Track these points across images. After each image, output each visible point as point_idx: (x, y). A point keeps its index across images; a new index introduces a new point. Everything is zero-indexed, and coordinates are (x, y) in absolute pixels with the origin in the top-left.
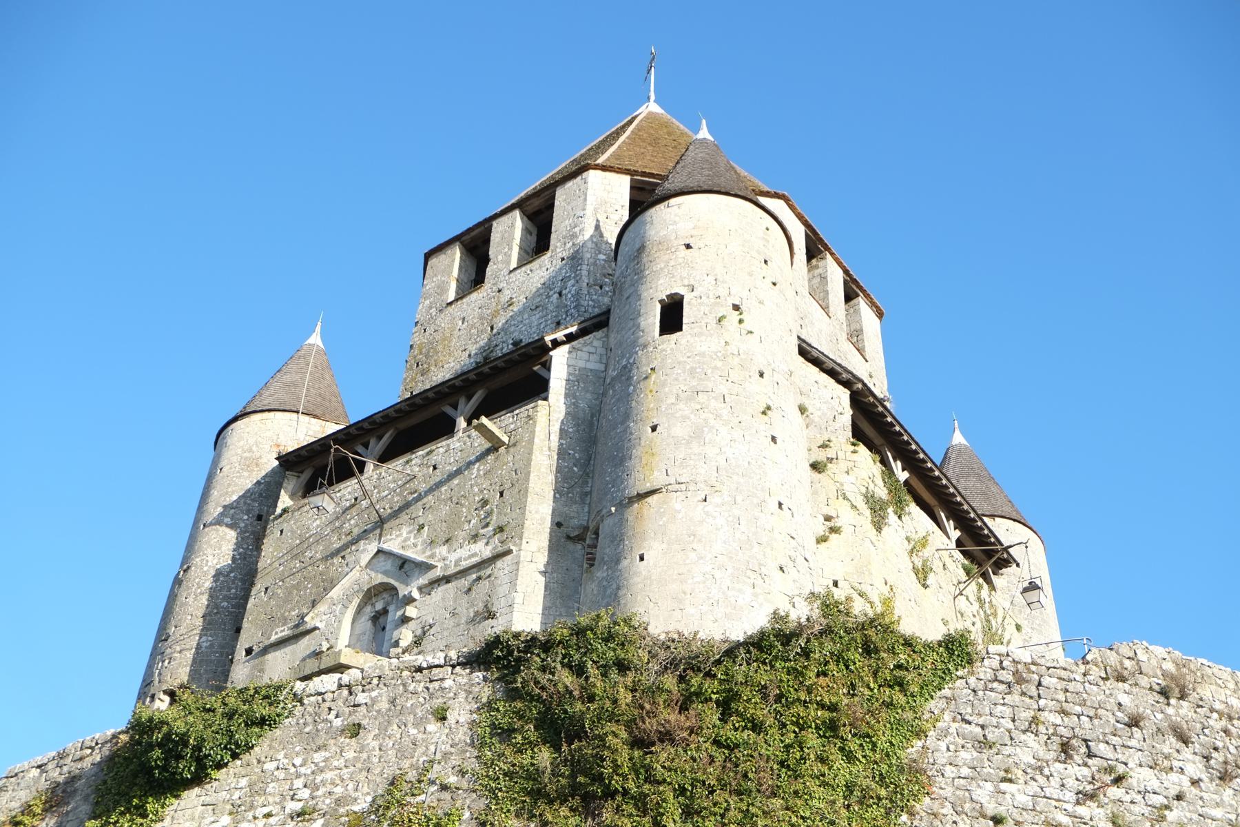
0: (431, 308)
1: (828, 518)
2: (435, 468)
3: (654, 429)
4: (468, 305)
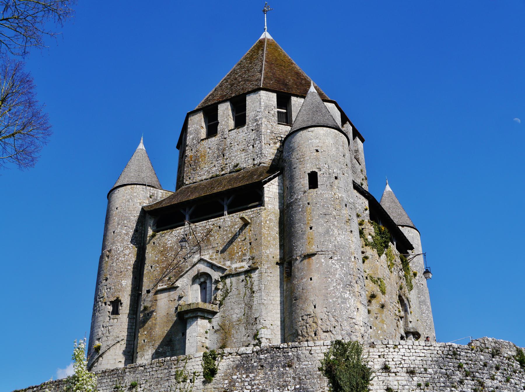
1: (363, 253)
2: (220, 227)
3: (311, 228)
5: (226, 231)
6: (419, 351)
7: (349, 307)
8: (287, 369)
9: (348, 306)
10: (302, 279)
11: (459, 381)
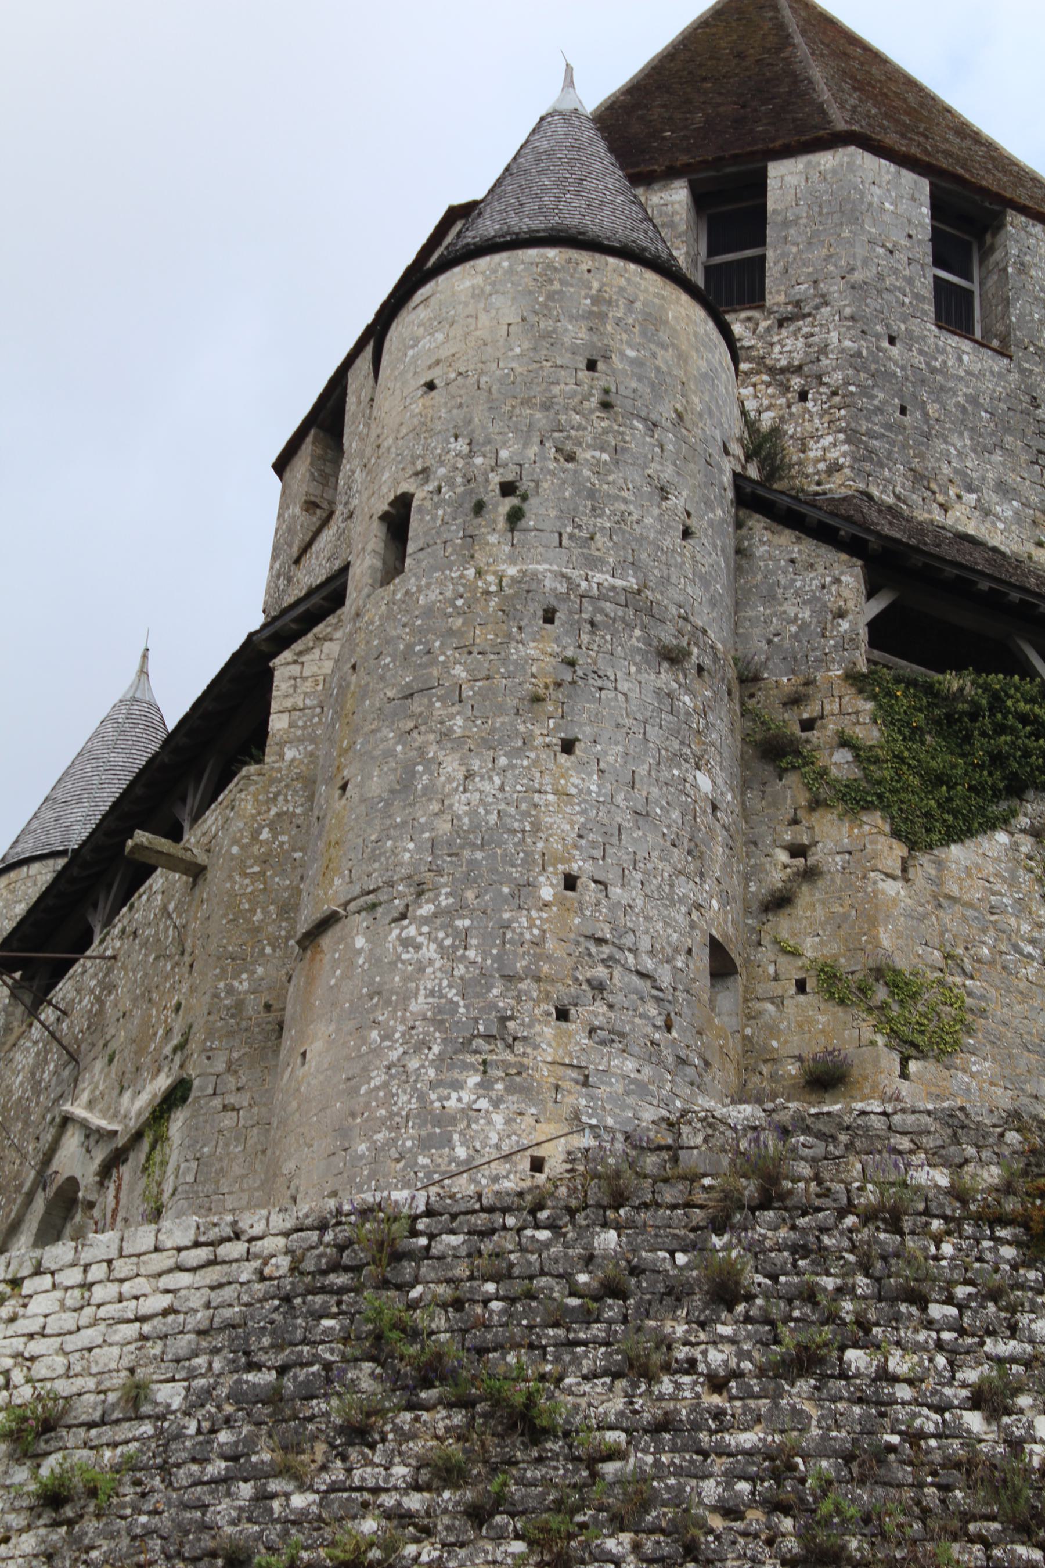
3: (344, 788)
9: (461, 1152)
11: (340, 1430)
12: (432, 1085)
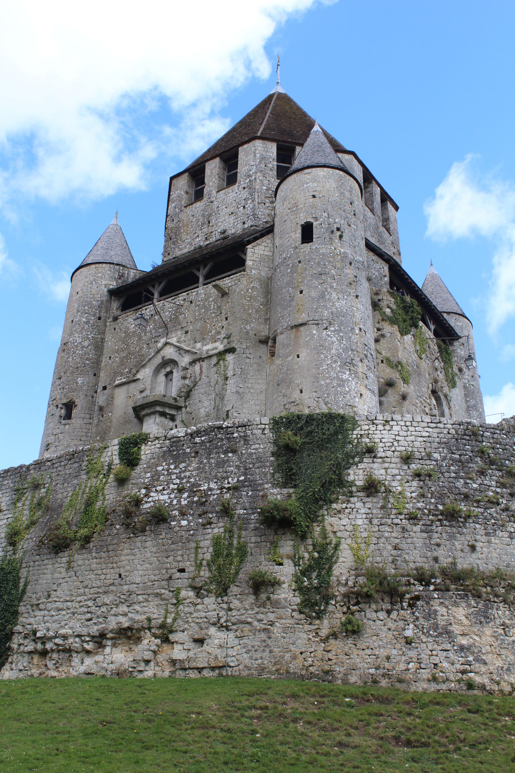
0: (175, 208)
1: (379, 330)
2: (191, 302)
3: (301, 292)
4: (196, 208)
5: (199, 306)
6: (421, 429)
7: (349, 392)
8: (230, 455)
9: (347, 389)
10: (287, 357)
11: (478, 471)
12: (339, 372)
